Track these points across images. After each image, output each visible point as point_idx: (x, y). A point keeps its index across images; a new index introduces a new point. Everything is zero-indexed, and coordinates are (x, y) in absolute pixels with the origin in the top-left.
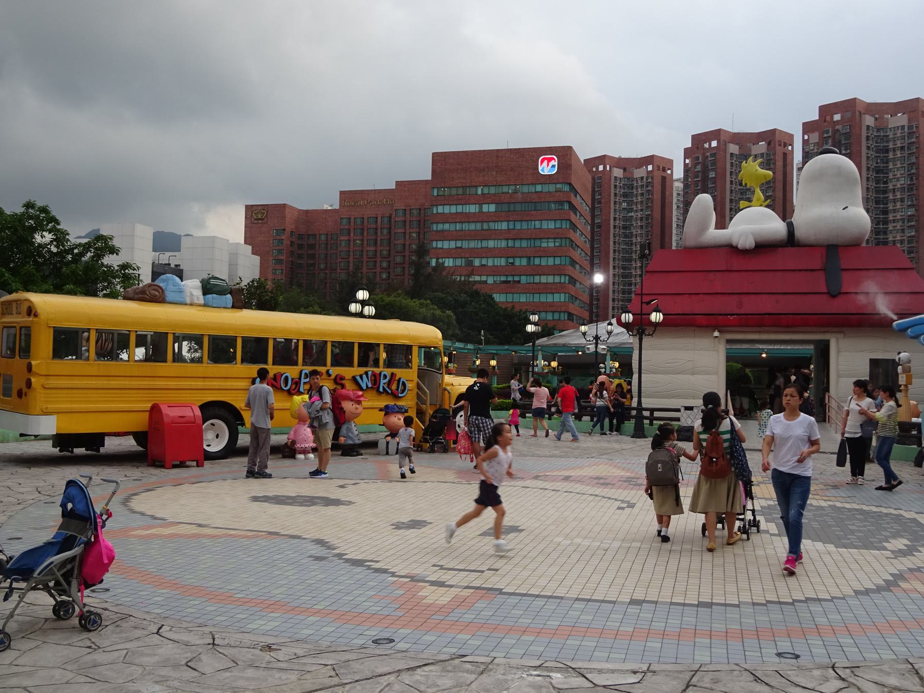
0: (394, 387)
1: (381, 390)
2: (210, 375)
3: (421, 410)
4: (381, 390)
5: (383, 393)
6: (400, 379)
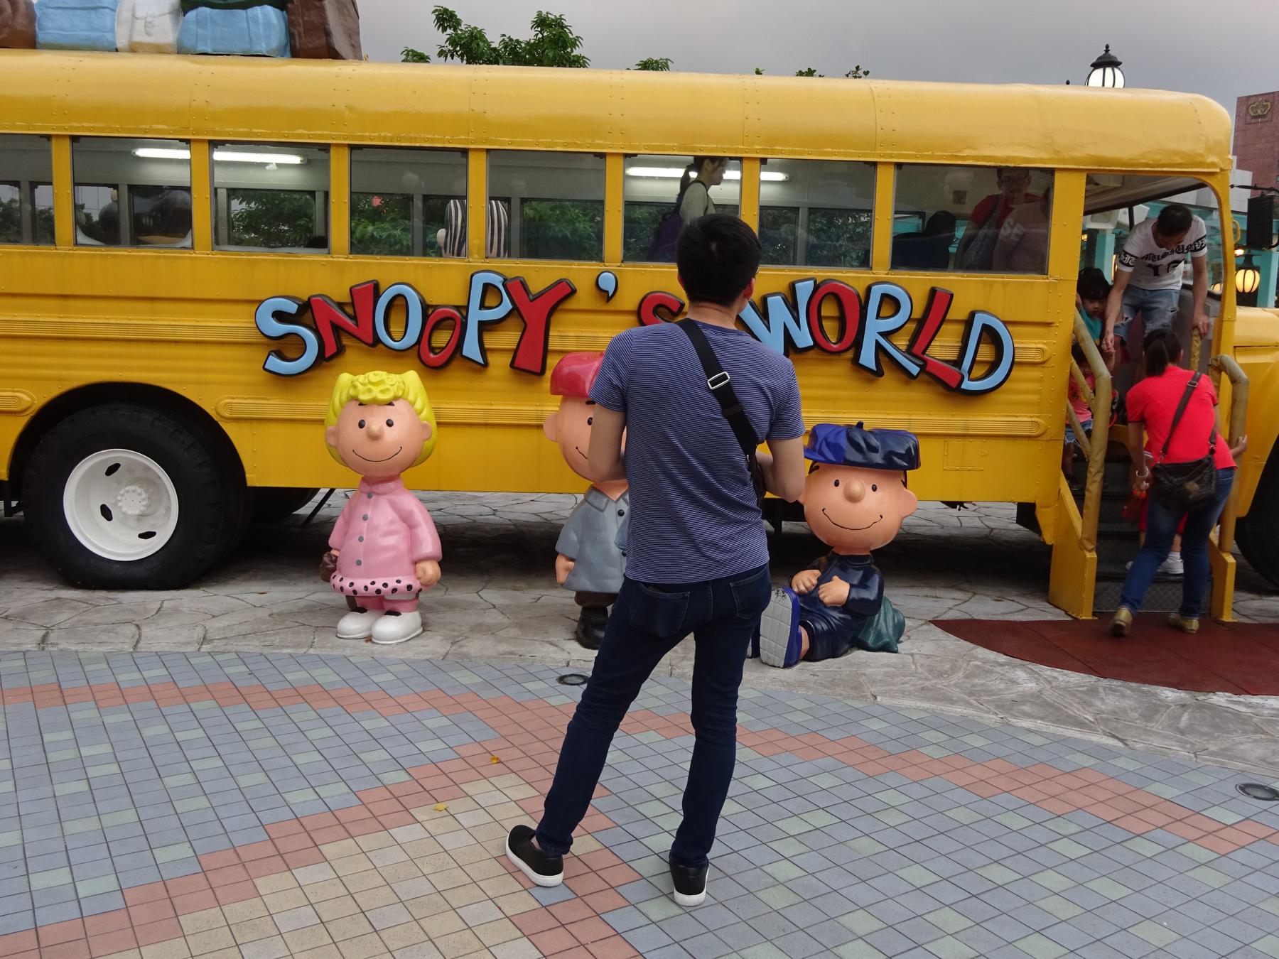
0: (943, 347)
1: (868, 357)
2: (164, 295)
3: (1122, 445)
4: (868, 357)
5: (879, 373)
6: (972, 315)
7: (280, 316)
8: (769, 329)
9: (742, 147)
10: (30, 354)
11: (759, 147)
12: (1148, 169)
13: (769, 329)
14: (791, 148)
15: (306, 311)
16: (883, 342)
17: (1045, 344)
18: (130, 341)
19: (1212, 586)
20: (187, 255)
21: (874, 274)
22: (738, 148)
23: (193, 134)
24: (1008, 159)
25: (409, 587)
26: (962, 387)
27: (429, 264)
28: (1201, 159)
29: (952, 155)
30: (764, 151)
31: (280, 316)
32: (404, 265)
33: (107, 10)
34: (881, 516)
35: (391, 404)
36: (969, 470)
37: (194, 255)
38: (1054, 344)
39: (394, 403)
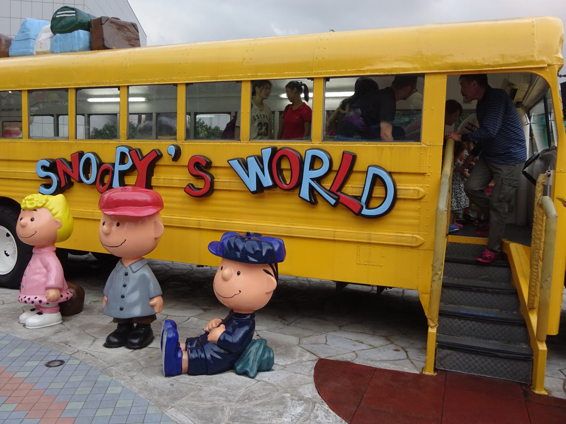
7: (44, 168)
8: (248, 176)
9: (241, 75)
10: (5, 186)
11: (250, 74)
12: (490, 69)
13: (248, 176)
14: (266, 74)
15: (53, 167)
16: (314, 184)
17: (421, 187)
18: (24, 180)
19: (533, 365)
20: (20, 141)
21: (313, 144)
22: (239, 76)
23: (22, 88)
24: (392, 70)
25: (40, 301)
26: (362, 213)
27: (103, 143)
28: (532, 59)
29: (357, 70)
30: (252, 76)
31: (44, 168)
32: (93, 143)
33: (31, 40)
34: (240, 291)
35: (35, 210)
36: (373, 265)
37: (22, 141)
38: (428, 187)
39: (37, 209)
